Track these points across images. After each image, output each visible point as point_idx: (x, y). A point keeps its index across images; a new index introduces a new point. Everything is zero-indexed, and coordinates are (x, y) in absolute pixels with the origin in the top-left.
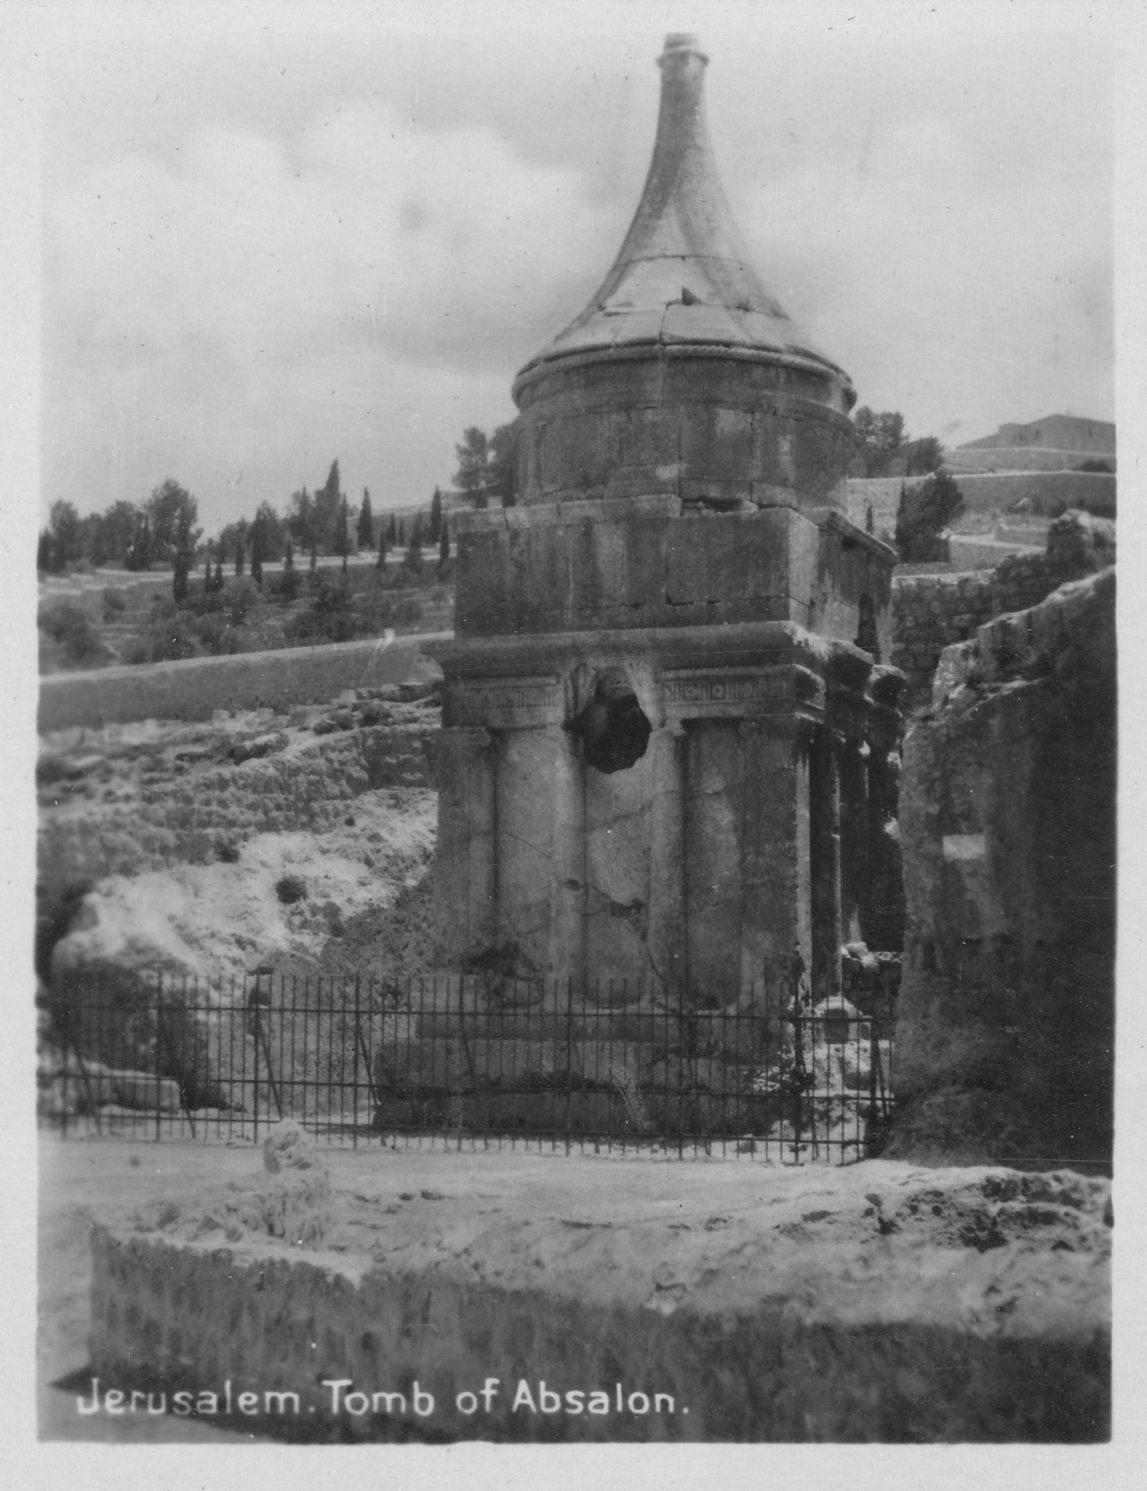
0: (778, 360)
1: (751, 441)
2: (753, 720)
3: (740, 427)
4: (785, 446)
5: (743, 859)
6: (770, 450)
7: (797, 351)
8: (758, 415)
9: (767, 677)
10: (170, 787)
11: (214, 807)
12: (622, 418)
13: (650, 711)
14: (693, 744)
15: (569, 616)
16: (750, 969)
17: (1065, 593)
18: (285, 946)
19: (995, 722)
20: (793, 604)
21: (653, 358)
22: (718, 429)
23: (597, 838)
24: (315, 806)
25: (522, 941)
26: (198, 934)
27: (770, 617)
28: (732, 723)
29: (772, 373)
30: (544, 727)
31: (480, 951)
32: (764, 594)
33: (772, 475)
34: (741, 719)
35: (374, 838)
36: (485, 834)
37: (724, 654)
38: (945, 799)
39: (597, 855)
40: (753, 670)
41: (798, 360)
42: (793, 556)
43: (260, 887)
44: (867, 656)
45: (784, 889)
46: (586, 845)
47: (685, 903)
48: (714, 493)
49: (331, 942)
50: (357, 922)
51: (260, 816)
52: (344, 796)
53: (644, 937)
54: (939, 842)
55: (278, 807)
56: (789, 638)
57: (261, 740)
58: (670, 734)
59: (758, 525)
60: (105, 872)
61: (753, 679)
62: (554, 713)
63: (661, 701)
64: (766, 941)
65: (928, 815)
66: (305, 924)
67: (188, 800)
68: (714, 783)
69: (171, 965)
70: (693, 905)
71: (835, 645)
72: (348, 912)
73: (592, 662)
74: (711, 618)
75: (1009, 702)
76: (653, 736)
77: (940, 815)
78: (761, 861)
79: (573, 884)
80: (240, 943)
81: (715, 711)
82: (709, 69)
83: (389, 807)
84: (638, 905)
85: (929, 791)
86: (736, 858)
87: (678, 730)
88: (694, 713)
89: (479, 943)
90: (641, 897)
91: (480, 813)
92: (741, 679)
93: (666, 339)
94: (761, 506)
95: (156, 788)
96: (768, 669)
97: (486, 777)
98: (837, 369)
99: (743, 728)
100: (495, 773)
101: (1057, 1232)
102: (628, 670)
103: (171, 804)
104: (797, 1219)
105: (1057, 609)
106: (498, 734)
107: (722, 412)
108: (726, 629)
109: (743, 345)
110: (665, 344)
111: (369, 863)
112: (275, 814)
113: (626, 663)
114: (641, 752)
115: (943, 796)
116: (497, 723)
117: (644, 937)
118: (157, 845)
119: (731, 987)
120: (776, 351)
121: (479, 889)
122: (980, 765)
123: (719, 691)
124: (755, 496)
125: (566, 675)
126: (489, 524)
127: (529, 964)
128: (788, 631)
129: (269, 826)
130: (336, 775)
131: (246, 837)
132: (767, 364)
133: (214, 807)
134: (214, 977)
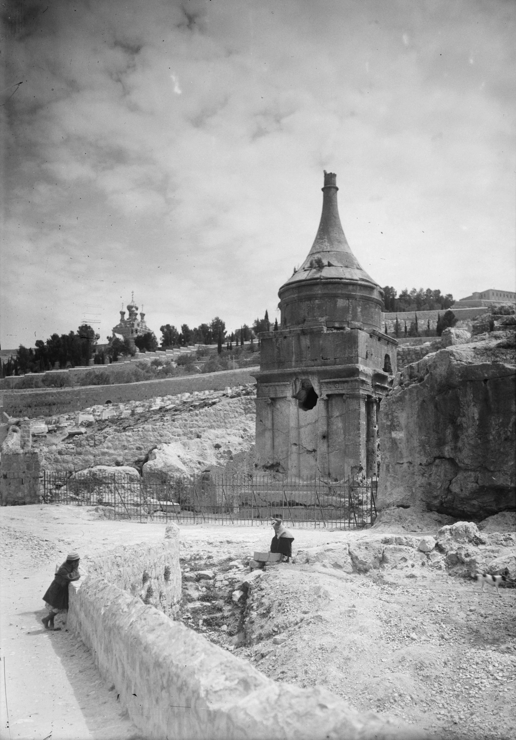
0: (357, 283)
1: (348, 308)
2: (348, 394)
3: (344, 305)
4: (359, 310)
5: (345, 437)
8: (350, 301)
9: (352, 381)
10: (180, 417)
11: (195, 422)
12: (309, 303)
13: (317, 392)
14: (330, 402)
15: (293, 364)
16: (347, 470)
17: (428, 357)
18: (215, 464)
19: (407, 397)
20: (360, 359)
21: (317, 284)
22: (338, 306)
23: (302, 430)
24: (226, 421)
25: (281, 462)
26: (187, 461)
27: (352, 363)
28: (342, 395)
29: (355, 287)
30: (286, 397)
31: (269, 465)
32: (351, 356)
33: (355, 318)
34: (344, 394)
35: (245, 430)
37: (338, 374)
38: (392, 420)
39: (303, 436)
40: (347, 379)
41: (363, 283)
42: (359, 344)
43: (208, 444)
44: (386, 374)
45: (357, 445)
46: (299, 432)
47: (328, 450)
48: (337, 325)
49: (229, 462)
50: (238, 456)
51: (209, 424)
53: (316, 460)
54: (390, 433)
55: (214, 421)
56: (358, 369)
57: (214, 400)
58: (323, 399)
59: (350, 334)
60: (160, 442)
61: (347, 382)
62: (289, 393)
63: (320, 388)
64: (352, 462)
65: (387, 425)
66: (222, 457)
67: (186, 420)
68: (336, 413)
69: (178, 470)
70: (330, 450)
71: (375, 370)
72: (234, 453)
73: (300, 377)
74: (335, 364)
75: (411, 391)
76: (318, 399)
77: (391, 426)
78: (350, 437)
79: (295, 444)
80: (199, 463)
81: (336, 392)
82: (338, 192)
83: (250, 420)
84: (314, 451)
85: (387, 418)
86: (343, 436)
87: (326, 398)
88: (330, 392)
89: (268, 462)
90: (315, 448)
91: (269, 424)
92: (344, 382)
93: (322, 277)
94: (352, 329)
95: (176, 417)
96: (352, 378)
97: (269, 412)
98: (376, 285)
99: (344, 397)
100: (273, 412)
101: (403, 554)
102: (311, 380)
103: (180, 421)
104: (322, 551)
105: (426, 362)
106: (272, 399)
107: (339, 300)
111: (242, 437)
112: (214, 424)
113: (310, 377)
115: (391, 420)
116: (272, 396)
117: (316, 460)
118: (176, 434)
119: (342, 474)
121: (268, 446)
122: (402, 409)
123: (337, 385)
124: (350, 326)
125: (293, 381)
126: (269, 336)
127: (283, 468)
128: (357, 367)
129: (211, 427)
130: (233, 411)
131: (204, 431)
132: (354, 284)
133: (195, 422)
134: (192, 474)
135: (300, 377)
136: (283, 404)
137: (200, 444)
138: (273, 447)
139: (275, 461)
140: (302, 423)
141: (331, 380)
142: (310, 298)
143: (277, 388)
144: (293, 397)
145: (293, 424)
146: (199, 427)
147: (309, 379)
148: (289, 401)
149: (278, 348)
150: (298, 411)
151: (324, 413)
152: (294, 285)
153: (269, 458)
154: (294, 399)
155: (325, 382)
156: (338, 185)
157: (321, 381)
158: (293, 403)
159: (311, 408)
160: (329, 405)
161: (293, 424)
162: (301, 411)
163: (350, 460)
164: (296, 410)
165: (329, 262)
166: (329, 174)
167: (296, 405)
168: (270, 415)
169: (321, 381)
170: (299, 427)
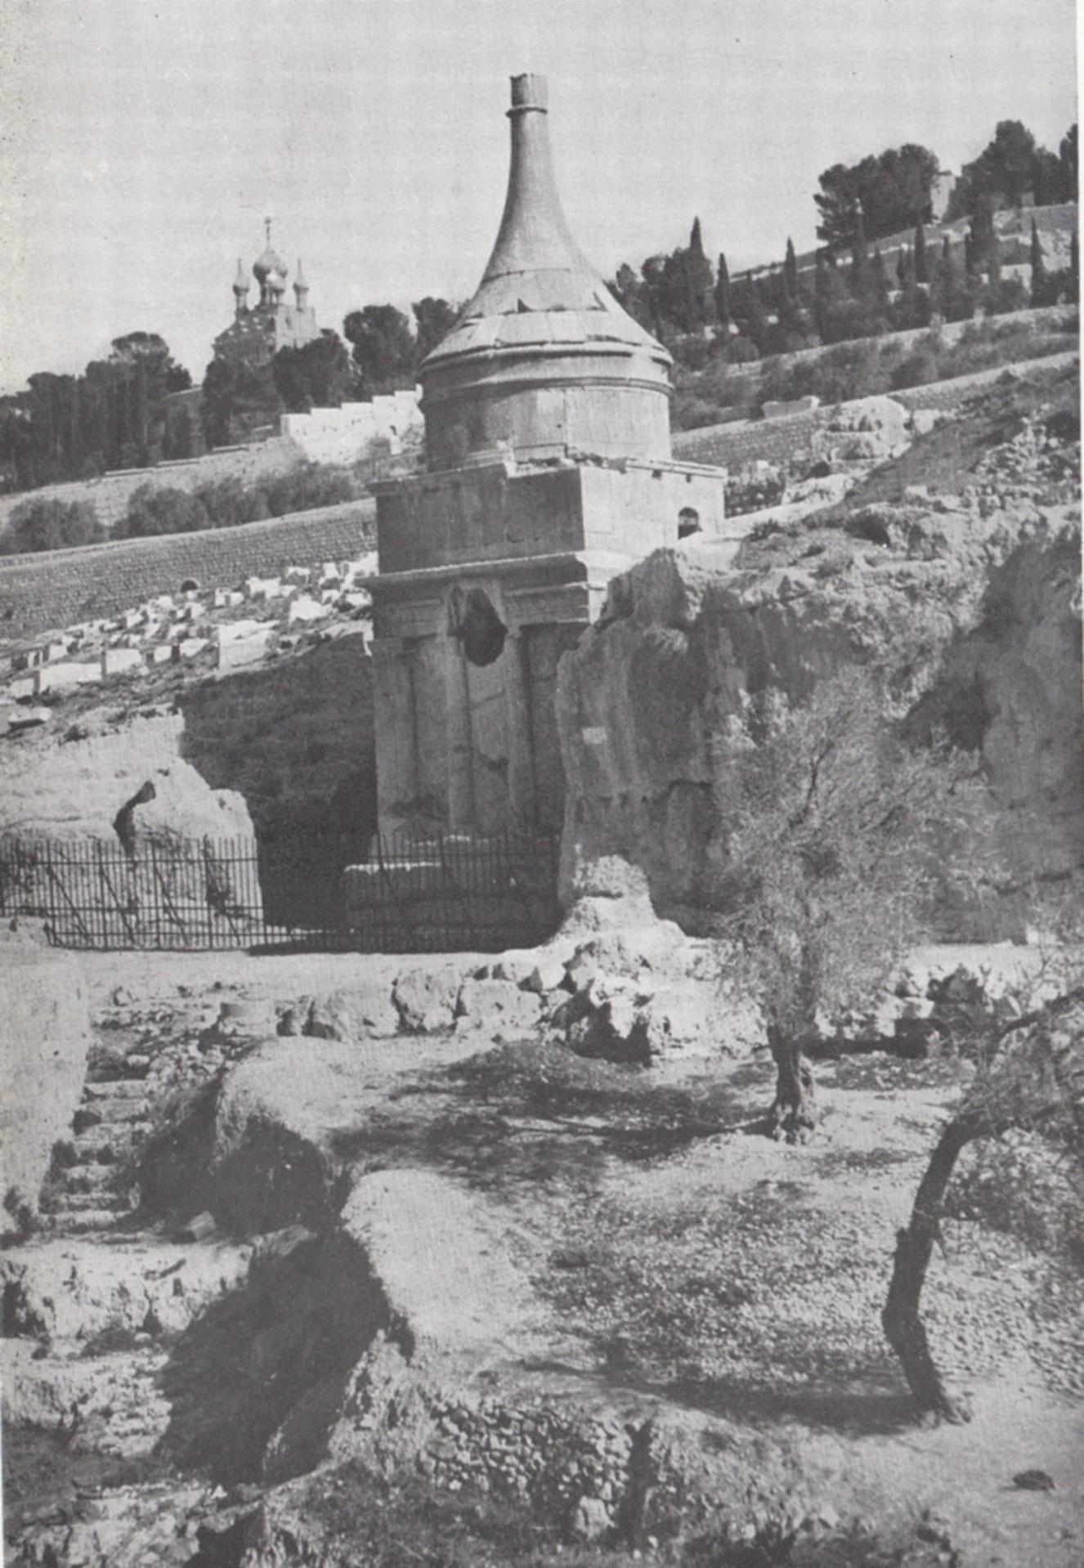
7: (599, 339)
13: (503, 619)
62: (442, 626)
63: (507, 612)
100: (411, 671)
108: (510, 560)
109: (554, 342)
114: (499, 650)
120: (581, 343)
125: (446, 597)
140: (477, 696)
141: (528, 591)
144: (451, 633)
145: (452, 700)
150: (464, 667)
151: (515, 673)
152: (440, 364)
154: (453, 639)
155: (515, 597)
157: (510, 594)
161: (452, 700)
162: (472, 668)
164: (458, 668)
167: (458, 653)
168: (406, 684)
170: (468, 708)
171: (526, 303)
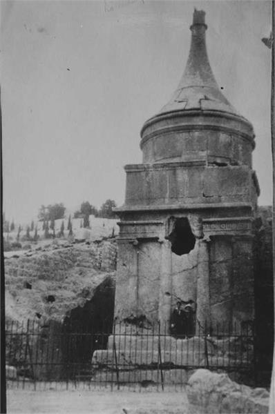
3: (227, 140)
6: (236, 147)
12: (187, 134)
13: (196, 233)
15: (167, 200)
31: (132, 318)
36: (134, 276)
46: (172, 280)
52: (66, 270)
58: (205, 241)
62: (161, 233)
63: (201, 229)
79: (168, 294)
87: (209, 240)
89: (132, 315)
90: (192, 299)
92: (231, 222)
102: (189, 218)
110: (203, 111)
131: (34, 281)
135: (176, 216)
136: (151, 247)
137: (31, 295)
138: (138, 298)
139: (139, 314)
142: (189, 129)
143: (147, 227)
144: (166, 238)
146: (30, 275)
147: (186, 219)
148: (161, 243)
149: (148, 183)
151: (204, 258)
153: (133, 310)
156: (206, 23)
158: (167, 246)
159: (188, 252)
160: (211, 249)
163: (240, 313)
165: (205, 97)
166: (199, 12)
169: (204, 220)
170: (172, 274)
171: (208, 96)
